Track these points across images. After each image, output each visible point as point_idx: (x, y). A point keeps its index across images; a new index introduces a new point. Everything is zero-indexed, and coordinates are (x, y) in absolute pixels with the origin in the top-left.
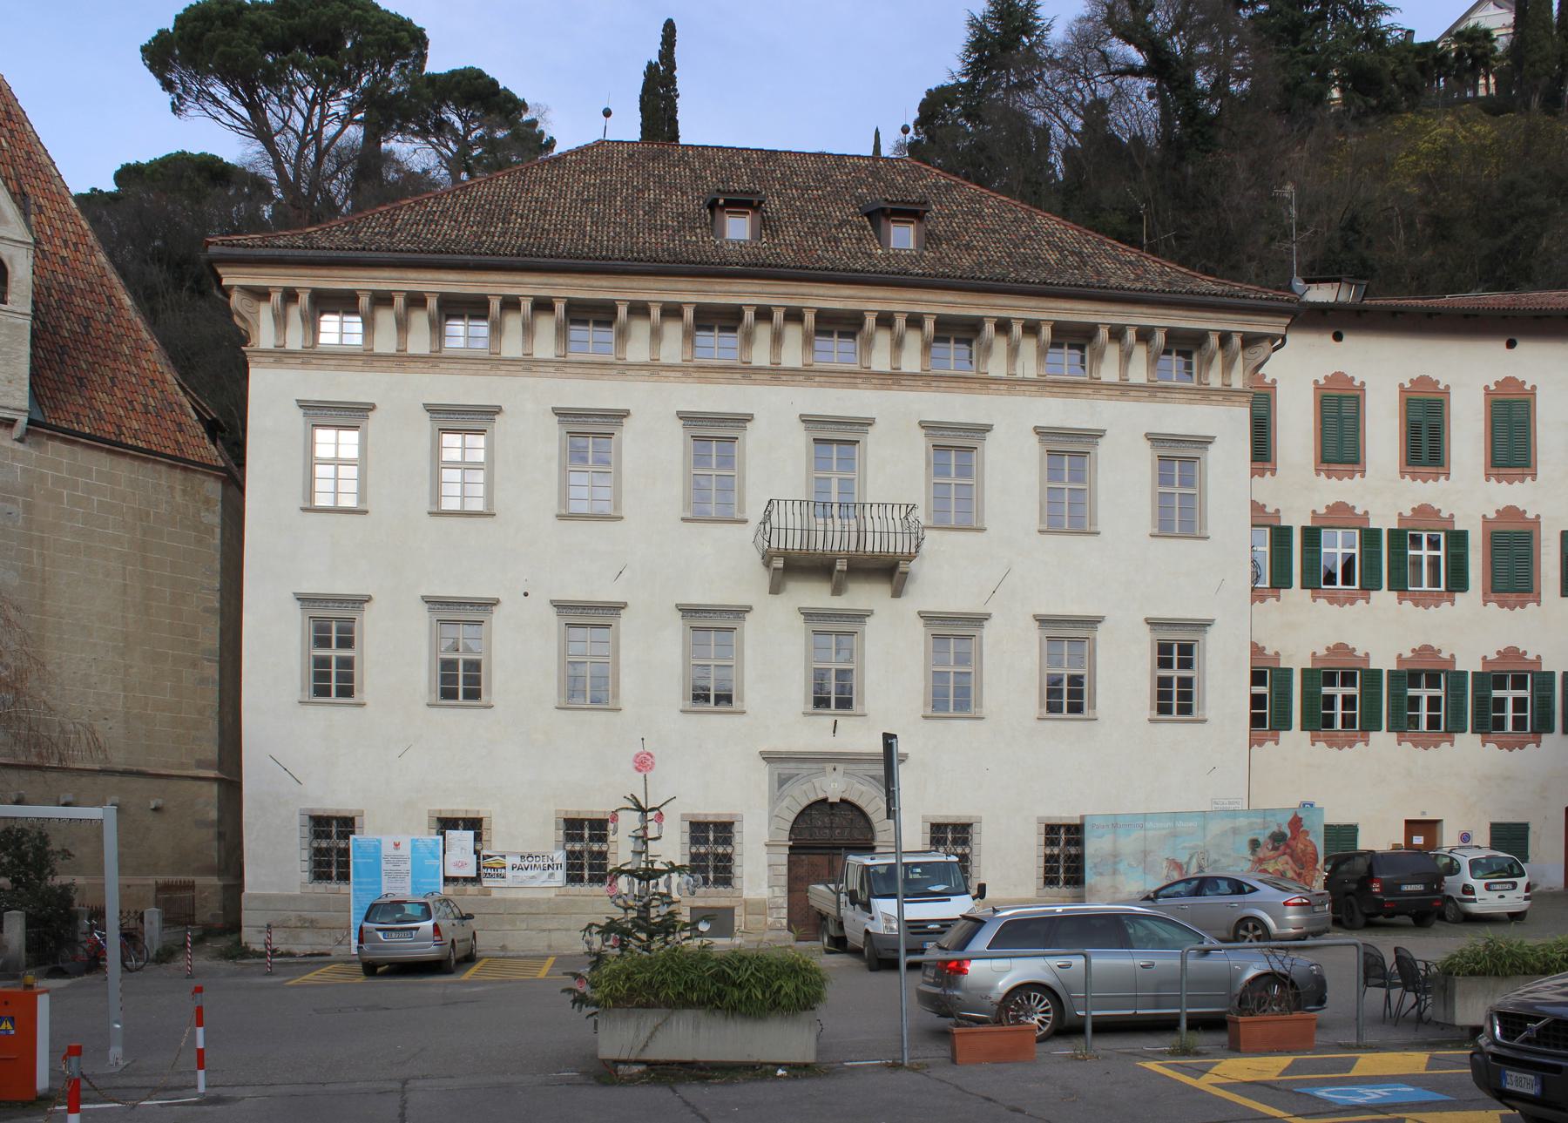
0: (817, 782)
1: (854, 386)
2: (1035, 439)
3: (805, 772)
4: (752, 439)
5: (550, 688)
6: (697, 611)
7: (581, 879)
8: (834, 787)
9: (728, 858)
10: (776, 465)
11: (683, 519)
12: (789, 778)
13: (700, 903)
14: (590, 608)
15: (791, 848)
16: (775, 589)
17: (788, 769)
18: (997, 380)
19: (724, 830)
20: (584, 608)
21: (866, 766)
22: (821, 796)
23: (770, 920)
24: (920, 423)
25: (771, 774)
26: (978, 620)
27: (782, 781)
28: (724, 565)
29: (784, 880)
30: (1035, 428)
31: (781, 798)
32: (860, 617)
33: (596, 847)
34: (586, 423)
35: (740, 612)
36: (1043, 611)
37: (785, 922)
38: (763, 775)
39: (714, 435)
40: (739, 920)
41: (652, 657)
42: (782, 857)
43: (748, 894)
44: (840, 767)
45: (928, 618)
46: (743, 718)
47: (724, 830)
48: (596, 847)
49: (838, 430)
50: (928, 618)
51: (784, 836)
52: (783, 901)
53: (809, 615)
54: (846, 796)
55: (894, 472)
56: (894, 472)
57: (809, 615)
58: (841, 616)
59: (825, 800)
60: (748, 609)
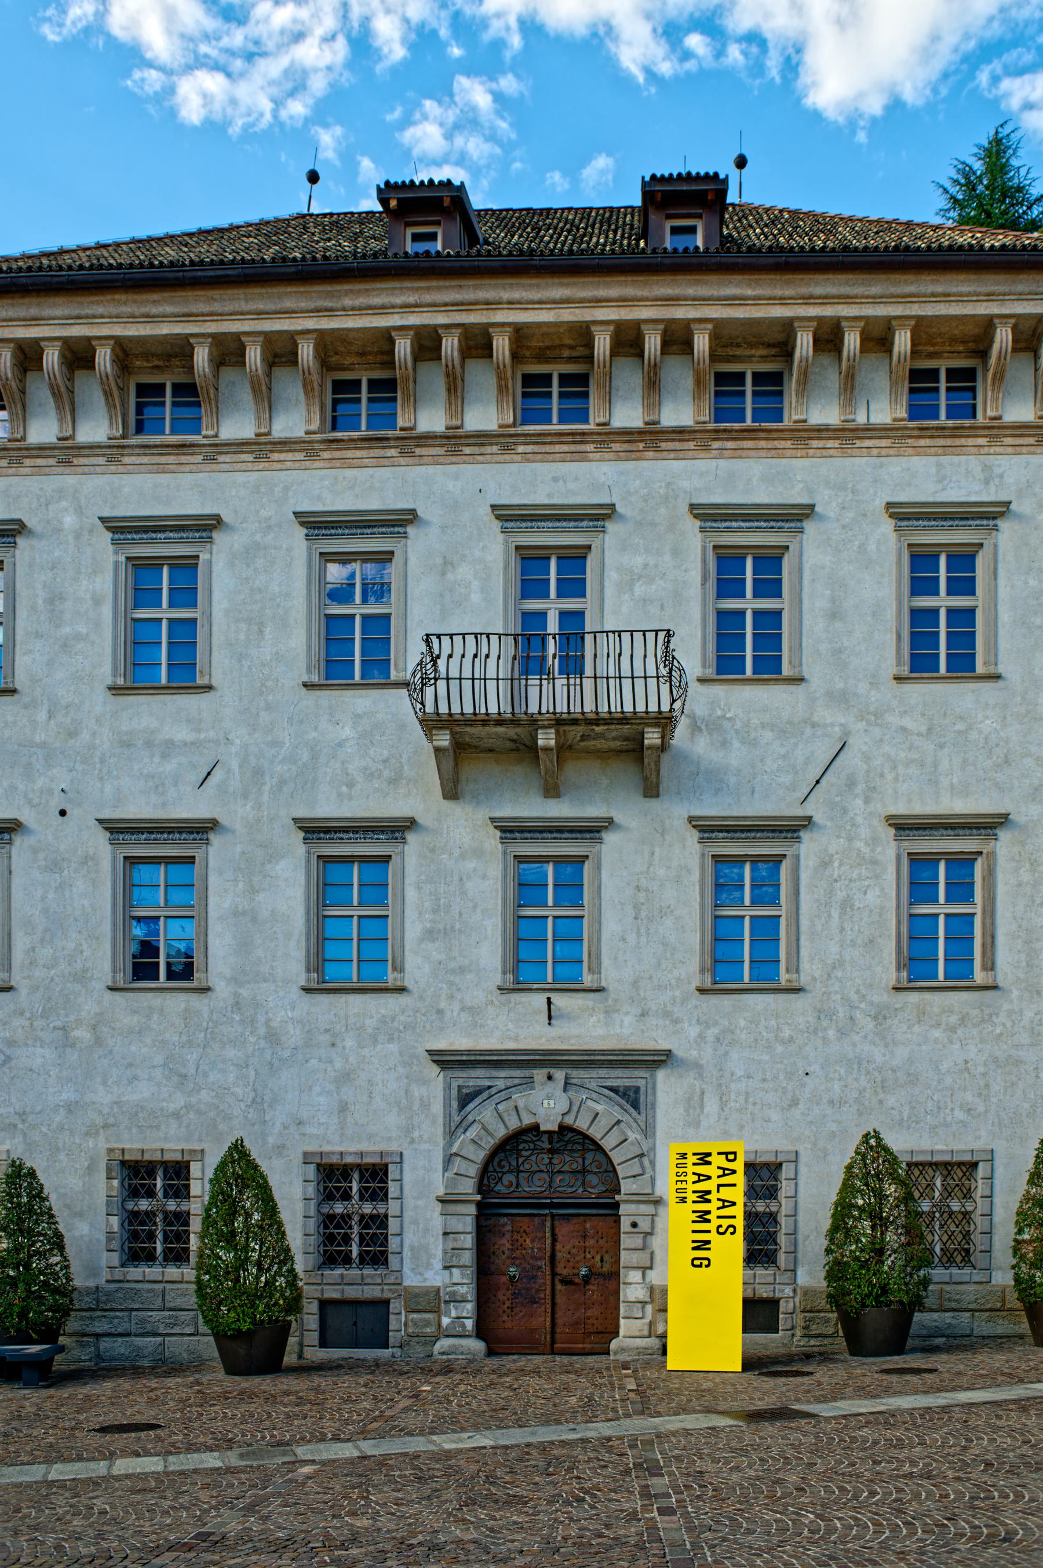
0: (519, 1098)
1: (582, 457)
2: (888, 526)
3: (501, 1084)
4: (416, 550)
5: (102, 956)
6: (328, 830)
7: (150, 1257)
8: (547, 1104)
9: (381, 1221)
10: (454, 590)
11: (305, 685)
12: (478, 1092)
13: (332, 1293)
14: (161, 830)
15: (479, 1205)
16: (452, 792)
17: (477, 1078)
18: (821, 432)
19: (376, 1176)
20: (151, 831)
21: (602, 1073)
22: (527, 1120)
23: (445, 1321)
24: (692, 507)
25: (448, 1087)
26: (792, 829)
27: (465, 1099)
28: (367, 751)
29: (468, 1258)
30: (889, 505)
31: (463, 1126)
32: (592, 831)
33: (172, 1205)
34: (152, 542)
35: (399, 829)
36: (900, 809)
37: (469, 1324)
38: (435, 1087)
39: (357, 544)
40: (399, 1322)
41: (255, 905)
42: (465, 1222)
43: (411, 1280)
44: (559, 1075)
45: (708, 829)
46: (403, 999)
47: (376, 1176)
48: (172, 1205)
49: (555, 531)
50: (708, 829)
51: (468, 1187)
52: (467, 1289)
53: (510, 831)
54: (569, 1120)
55: (650, 588)
56: (650, 588)
57: (510, 831)
58: (560, 830)
59: (535, 1128)
60: (410, 824)
